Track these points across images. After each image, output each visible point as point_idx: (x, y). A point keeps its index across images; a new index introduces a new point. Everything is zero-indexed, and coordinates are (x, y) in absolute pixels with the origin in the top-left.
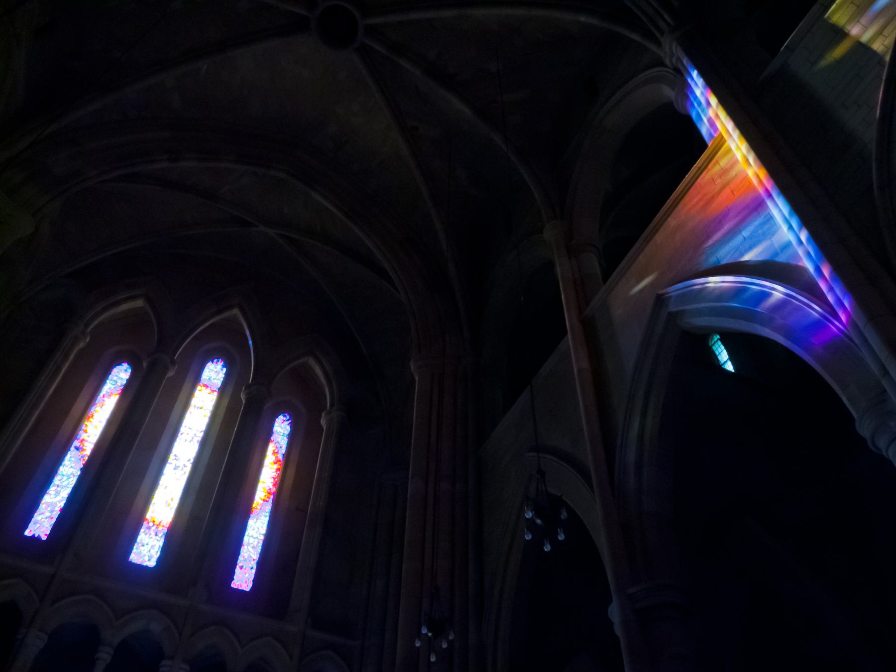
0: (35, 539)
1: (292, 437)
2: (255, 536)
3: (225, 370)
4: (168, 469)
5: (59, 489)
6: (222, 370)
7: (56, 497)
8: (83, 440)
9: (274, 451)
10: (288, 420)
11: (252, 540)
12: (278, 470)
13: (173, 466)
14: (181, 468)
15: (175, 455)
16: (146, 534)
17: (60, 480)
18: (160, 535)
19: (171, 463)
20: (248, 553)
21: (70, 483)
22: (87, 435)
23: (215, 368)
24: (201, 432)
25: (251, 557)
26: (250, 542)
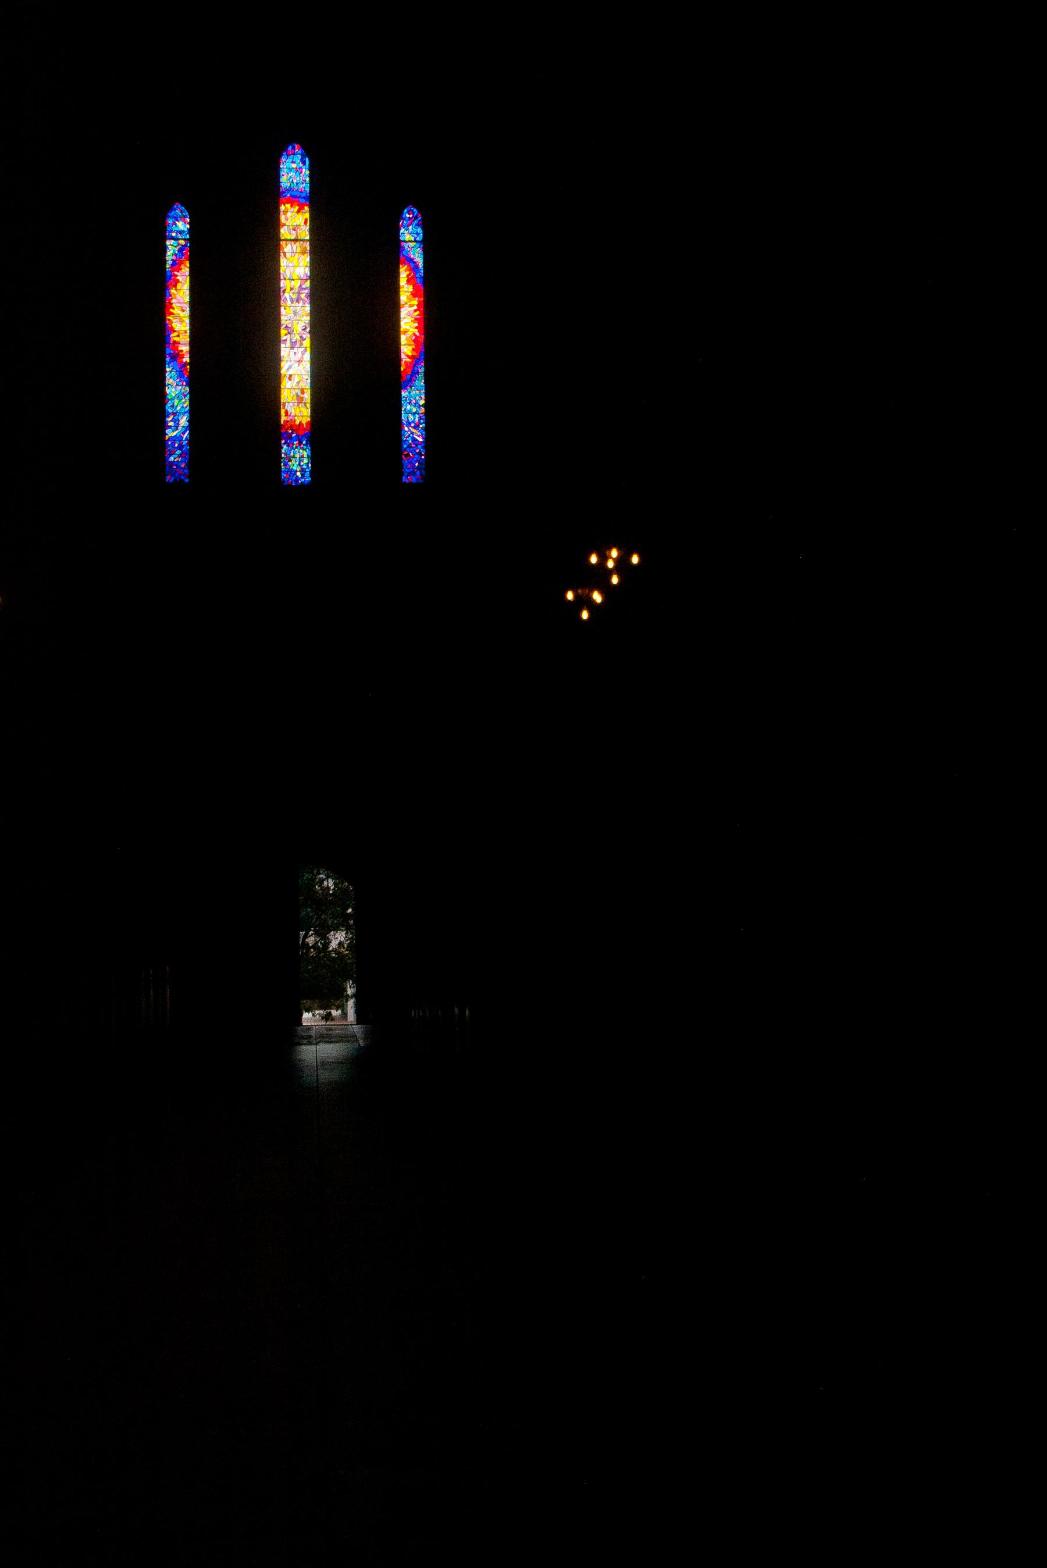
0: (178, 483)
1: (428, 245)
2: (414, 410)
3: (307, 160)
4: (285, 351)
5: (176, 417)
6: (304, 163)
7: (177, 429)
8: (175, 342)
9: (408, 276)
10: (416, 218)
11: (411, 418)
12: (419, 302)
13: (288, 344)
14: (298, 345)
15: (287, 327)
16: (288, 446)
17: (172, 406)
18: (304, 442)
19: (286, 340)
20: (411, 435)
21: (185, 405)
22: (175, 334)
23: (294, 162)
24: (307, 280)
25: (417, 440)
26: (410, 421)
